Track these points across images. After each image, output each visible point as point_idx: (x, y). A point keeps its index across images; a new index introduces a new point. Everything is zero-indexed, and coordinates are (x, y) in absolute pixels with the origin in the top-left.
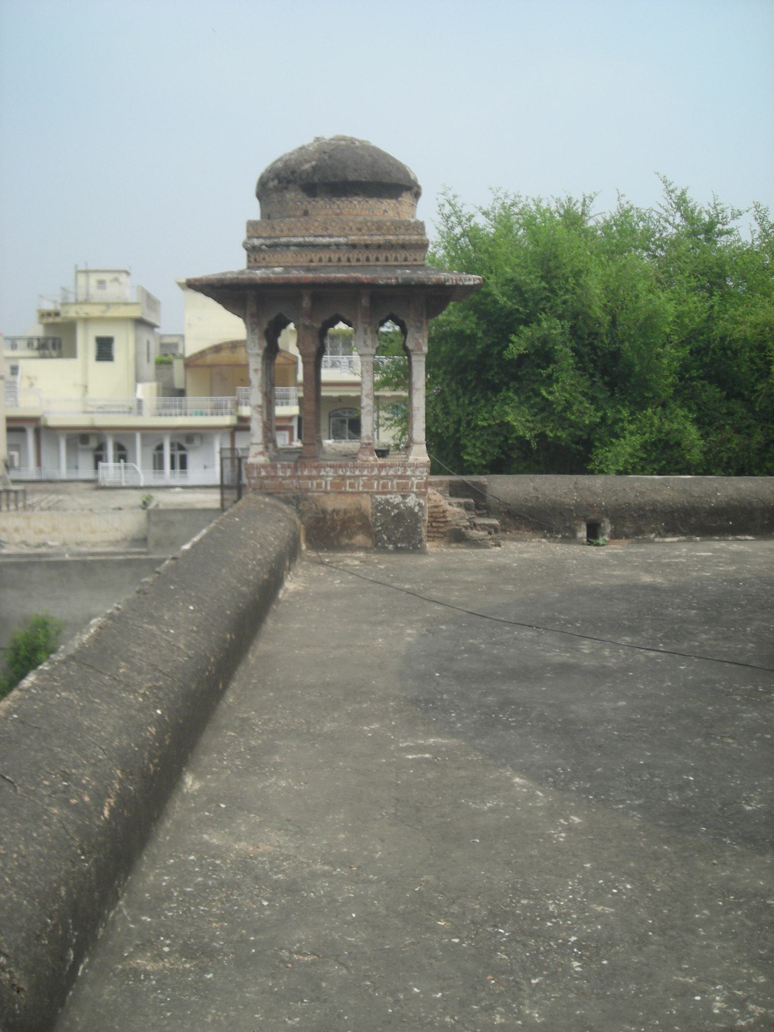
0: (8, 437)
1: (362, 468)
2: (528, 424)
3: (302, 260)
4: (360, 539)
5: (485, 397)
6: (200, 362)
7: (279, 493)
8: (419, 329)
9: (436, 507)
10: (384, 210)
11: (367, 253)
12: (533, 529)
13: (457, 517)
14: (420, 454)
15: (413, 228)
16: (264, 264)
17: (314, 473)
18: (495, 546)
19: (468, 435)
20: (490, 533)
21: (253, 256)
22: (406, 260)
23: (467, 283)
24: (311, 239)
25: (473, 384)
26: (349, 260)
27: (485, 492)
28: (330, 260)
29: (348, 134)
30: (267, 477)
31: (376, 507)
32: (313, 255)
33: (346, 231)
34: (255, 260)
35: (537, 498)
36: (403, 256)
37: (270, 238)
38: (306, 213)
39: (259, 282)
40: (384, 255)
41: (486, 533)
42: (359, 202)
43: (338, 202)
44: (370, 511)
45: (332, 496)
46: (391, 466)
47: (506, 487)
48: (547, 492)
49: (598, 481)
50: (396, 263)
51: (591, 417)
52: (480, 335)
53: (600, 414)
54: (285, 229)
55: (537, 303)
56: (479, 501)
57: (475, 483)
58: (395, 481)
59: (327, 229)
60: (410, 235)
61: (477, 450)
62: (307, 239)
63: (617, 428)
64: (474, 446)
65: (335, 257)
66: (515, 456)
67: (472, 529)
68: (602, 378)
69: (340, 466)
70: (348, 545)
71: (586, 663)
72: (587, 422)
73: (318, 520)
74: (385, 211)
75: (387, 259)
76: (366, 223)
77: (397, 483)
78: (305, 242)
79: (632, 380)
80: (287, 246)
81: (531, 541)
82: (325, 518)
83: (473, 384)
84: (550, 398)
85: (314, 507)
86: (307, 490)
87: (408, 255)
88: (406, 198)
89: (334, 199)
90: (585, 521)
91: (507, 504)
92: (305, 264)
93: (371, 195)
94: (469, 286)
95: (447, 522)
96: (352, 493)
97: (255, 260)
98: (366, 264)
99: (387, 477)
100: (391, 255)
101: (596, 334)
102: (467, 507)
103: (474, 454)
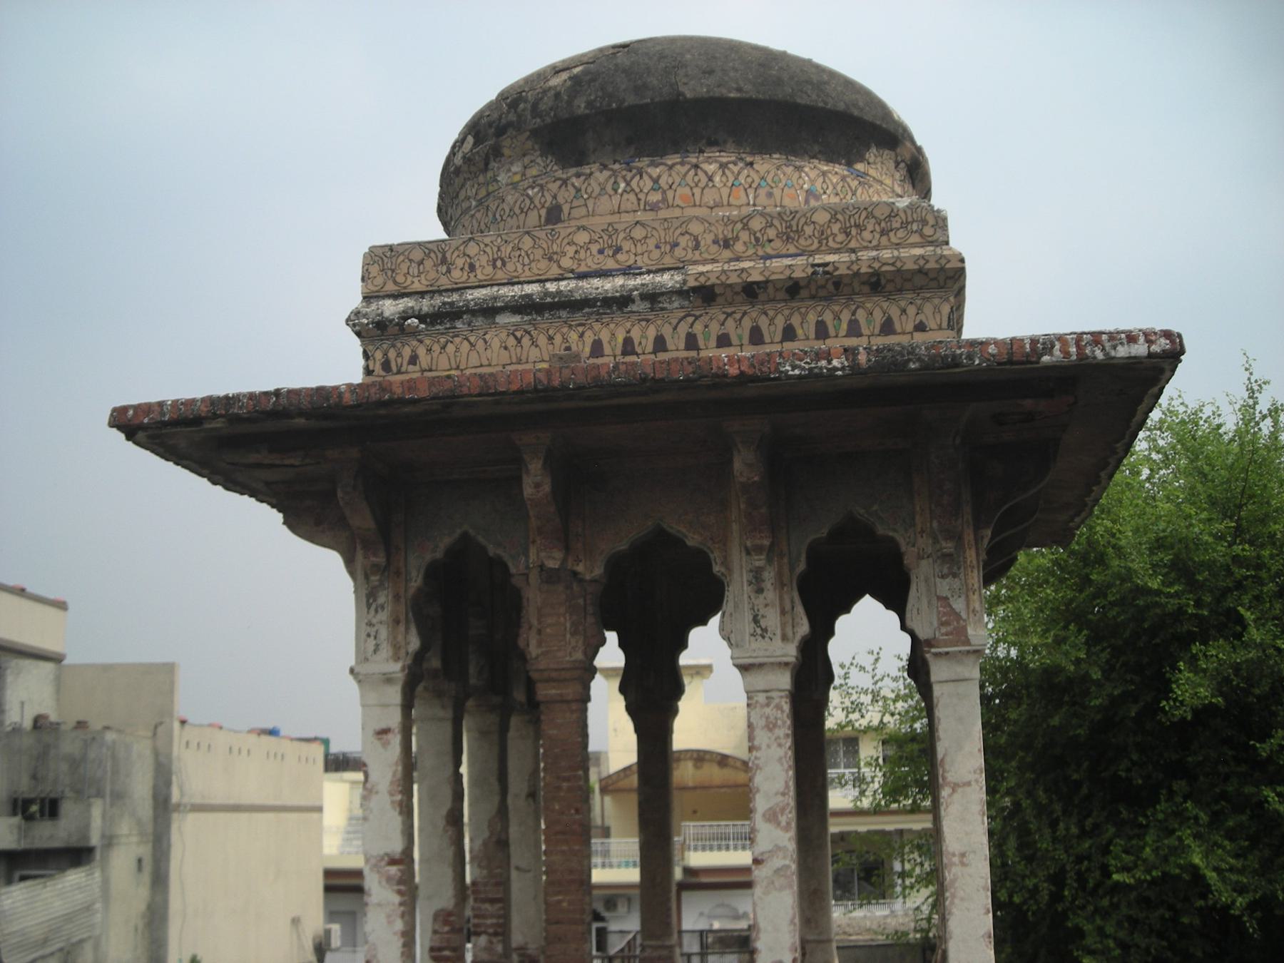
0: (326, 898)
2: (1234, 877)
3: (534, 354)
8: (951, 563)
15: (905, 225)
19: (1083, 908)
21: (379, 355)
23: (1122, 352)
25: (1084, 790)
32: (574, 336)
33: (678, 252)
34: (386, 366)
36: (878, 317)
39: (349, 399)
40: (812, 318)
42: (723, 166)
43: (655, 172)
52: (1096, 674)
59: (618, 250)
60: (898, 246)
61: (1111, 944)
62: (551, 287)
64: (1101, 931)
65: (644, 336)
74: (809, 193)
76: (745, 222)
78: (547, 294)
80: (489, 311)
87: (894, 312)
93: (763, 148)
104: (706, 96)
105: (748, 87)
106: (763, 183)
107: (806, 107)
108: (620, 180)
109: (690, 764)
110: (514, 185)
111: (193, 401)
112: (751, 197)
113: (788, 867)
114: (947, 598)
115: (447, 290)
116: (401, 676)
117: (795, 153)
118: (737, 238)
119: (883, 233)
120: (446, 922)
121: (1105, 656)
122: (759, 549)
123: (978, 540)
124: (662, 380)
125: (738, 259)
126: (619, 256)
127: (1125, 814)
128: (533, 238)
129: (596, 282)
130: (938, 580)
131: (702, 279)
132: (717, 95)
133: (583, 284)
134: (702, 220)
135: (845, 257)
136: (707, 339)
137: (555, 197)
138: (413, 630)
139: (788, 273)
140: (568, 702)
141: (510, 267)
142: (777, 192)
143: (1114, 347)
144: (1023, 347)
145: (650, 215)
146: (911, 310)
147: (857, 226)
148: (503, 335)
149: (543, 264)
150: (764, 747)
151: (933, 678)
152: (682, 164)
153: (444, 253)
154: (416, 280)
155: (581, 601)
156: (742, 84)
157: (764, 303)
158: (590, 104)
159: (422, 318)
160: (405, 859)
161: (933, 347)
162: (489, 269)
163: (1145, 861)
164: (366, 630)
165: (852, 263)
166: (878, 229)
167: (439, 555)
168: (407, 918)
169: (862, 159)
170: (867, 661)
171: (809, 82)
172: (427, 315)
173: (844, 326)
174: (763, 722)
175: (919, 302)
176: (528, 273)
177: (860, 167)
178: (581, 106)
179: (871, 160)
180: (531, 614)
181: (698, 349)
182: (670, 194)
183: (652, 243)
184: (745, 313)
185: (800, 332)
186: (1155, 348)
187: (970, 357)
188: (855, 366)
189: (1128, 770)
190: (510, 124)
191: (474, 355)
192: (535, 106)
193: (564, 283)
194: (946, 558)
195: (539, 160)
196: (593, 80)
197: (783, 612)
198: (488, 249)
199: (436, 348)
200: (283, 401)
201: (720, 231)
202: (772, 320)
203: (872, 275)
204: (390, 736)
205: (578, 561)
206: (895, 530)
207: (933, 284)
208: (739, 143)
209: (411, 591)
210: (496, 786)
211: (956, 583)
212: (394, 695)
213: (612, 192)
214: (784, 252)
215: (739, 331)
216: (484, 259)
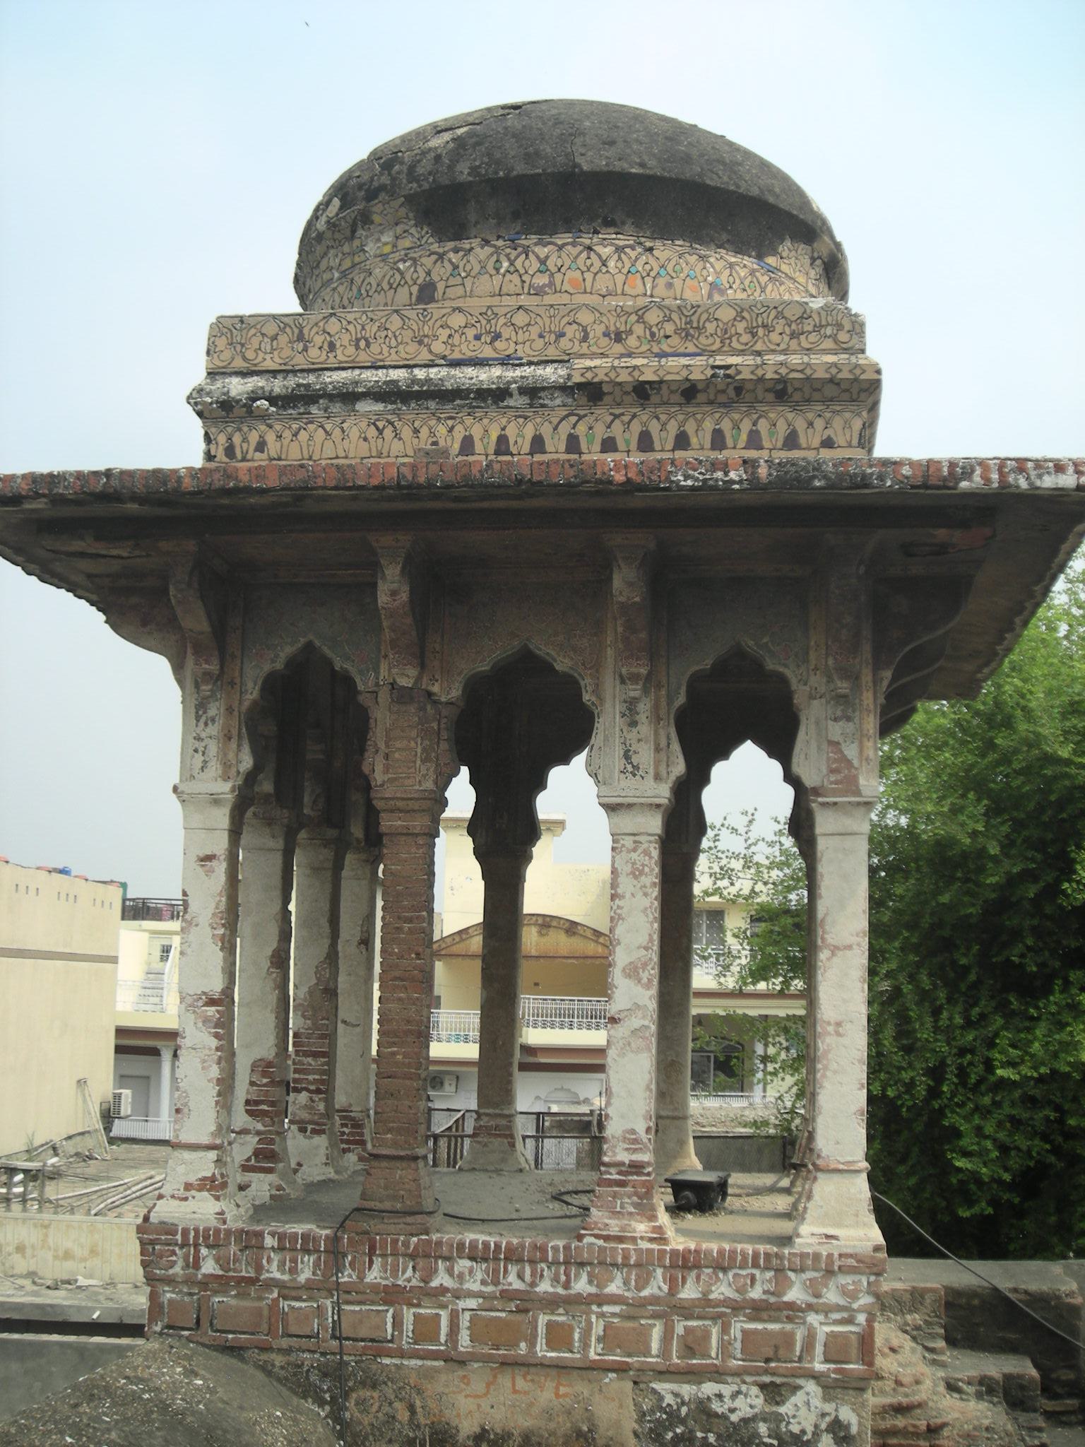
0: (116, 1059)
1: (603, 1265)
3: (397, 447)
5: (1003, 1007)
7: (265, 1349)
8: (845, 705)
9: (900, 1409)
11: (644, 419)
14: (841, 1212)
15: (818, 328)
17: (408, 1277)
21: (222, 439)
23: (1048, 482)
25: (972, 977)
27: (1075, 1332)
30: (220, 1283)
32: (442, 430)
33: (564, 343)
34: (230, 451)
39: (188, 485)
40: (709, 425)
42: (620, 250)
43: (543, 251)
45: (478, 1376)
46: (722, 1265)
52: (994, 849)
58: (739, 1326)
59: (497, 336)
61: (989, 1144)
62: (420, 374)
64: (979, 1131)
69: (513, 1256)
76: (640, 313)
77: (744, 1331)
78: (414, 381)
80: (348, 397)
83: (972, 977)
85: (404, 1416)
86: (378, 1346)
87: (800, 425)
93: (665, 232)
94: (1060, 493)
96: (560, 1368)
97: (230, 451)
99: (703, 1308)
102: (1012, 1395)
103: (982, 1153)
104: (605, 169)
105: (652, 163)
106: (663, 272)
107: (717, 189)
108: (502, 258)
109: (534, 930)
110: (383, 257)
111: (13, 477)
112: (649, 286)
113: (647, 1027)
114: (838, 743)
115: (302, 371)
116: (230, 797)
118: (630, 332)
119: (793, 335)
120: (264, 1074)
121: (1005, 829)
122: (634, 678)
123: (876, 682)
124: (540, 482)
125: (630, 355)
126: (497, 344)
127: (1015, 1004)
128: (402, 317)
129: (470, 371)
130: (830, 722)
131: (589, 375)
132: (618, 169)
133: (456, 372)
134: (593, 309)
135: (750, 360)
136: (590, 442)
137: (428, 273)
139: (684, 373)
140: (417, 835)
141: (375, 348)
142: (677, 283)
143: (1040, 476)
144: (940, 470)
145: (535, 300)
146: (819, 424)
147: (764, 326)
148: (364, 425)
149: (412, 348)
150: (628, 895)
151: (818, 830)
152: (574, 244)
153: (301, 329)
154: (268, 357)
155: (435, 725)
156: (646, 158)
157: (656, 405)
158: (474, 170)
159: (272, 400)
160: (223, 1000)
161: (841, 463)
162: (351, 350)
163: (1032, 1056)
164: (193, 746)
165: (757, 366)
166: (787, 330)
167: (279, 666)
168: (223, 1063)
169: (774, 252)
170: (740, 822)
171: (721, 161)
172: (279, 397)
173: (744, 437)
174: (628, 868)
175: (828, 415)
176: (394, 356)
177: (771, 260)
178: (463, 172)
179: (784, 254)
180: (378, 736)
181: (580, 453)
182: (558, 277)
183: (535, 331)
184: (634, 416)
185: (694, 441)
187: (881, 478)
188: (754, 481)
189: (1022, 956)
190: (382, 188)
191: (329, 444)
192: (412, 169)
193: (434, 370)
194: (842, 699)
195: (413, 230)
196: (478, 144)
197: (658, 749)
198: (351, 327)
199: (287, 434)
201: (613, 323)
202: (664, 425)
203: (778, 381)
204: (214, 863)
205: (435, 680)
206: (786, 666)
207: (846, 396)
208: (638, 225)
209: (246, 704)
210: (327, 930)
212: (221, 818)
213: (494, 272)
214: (682, 350)
215: (627, 435)
216: (346, 338)
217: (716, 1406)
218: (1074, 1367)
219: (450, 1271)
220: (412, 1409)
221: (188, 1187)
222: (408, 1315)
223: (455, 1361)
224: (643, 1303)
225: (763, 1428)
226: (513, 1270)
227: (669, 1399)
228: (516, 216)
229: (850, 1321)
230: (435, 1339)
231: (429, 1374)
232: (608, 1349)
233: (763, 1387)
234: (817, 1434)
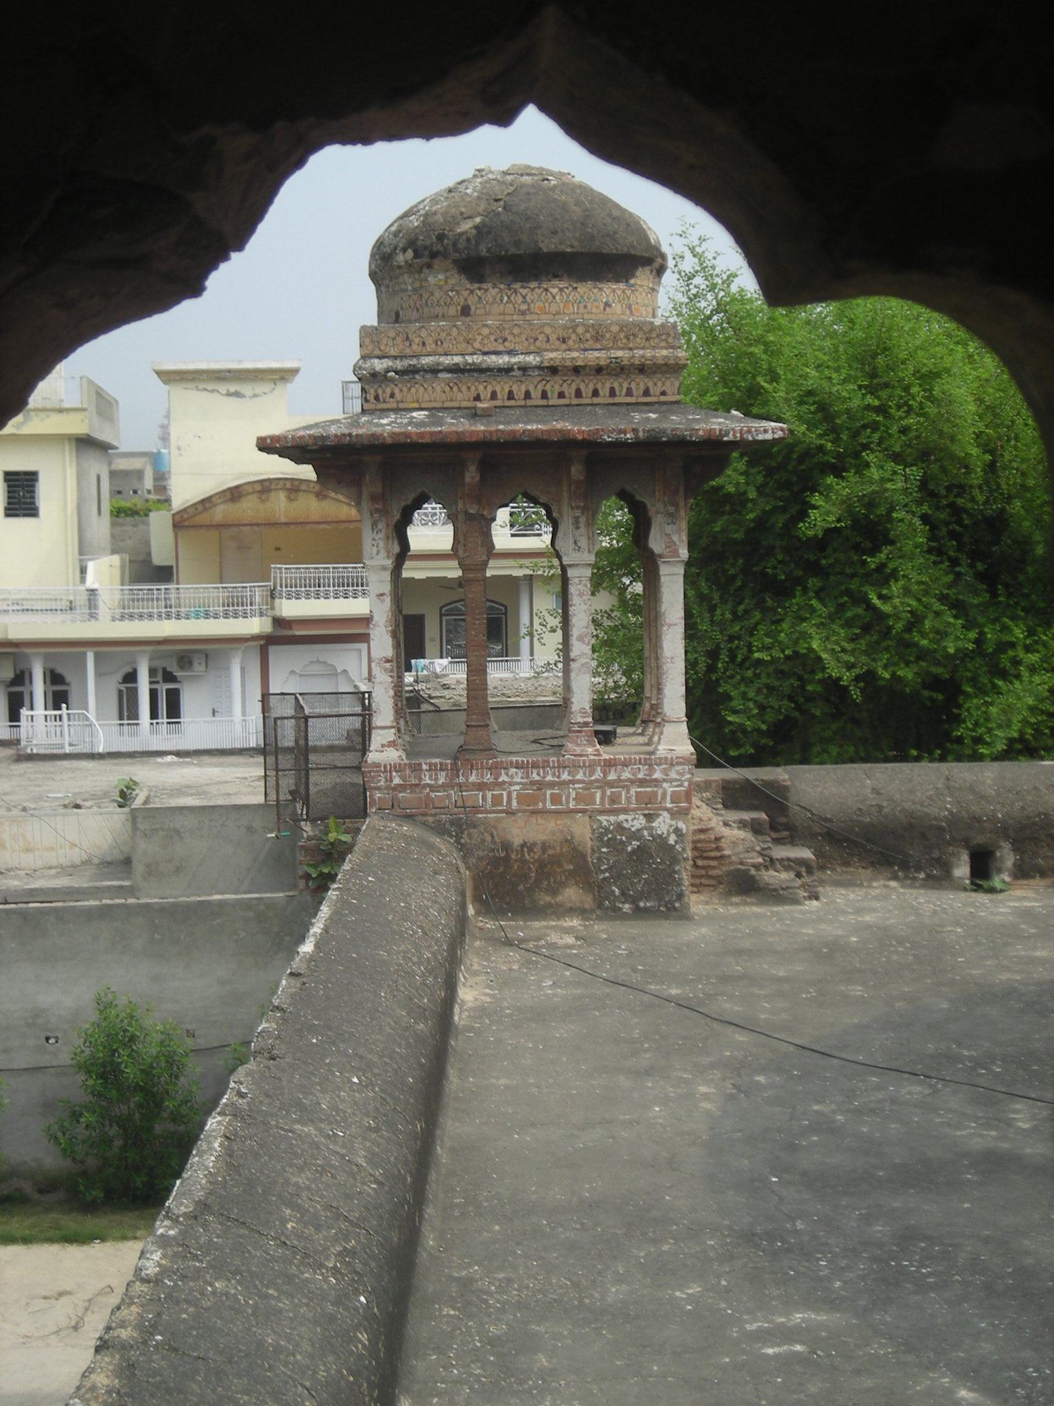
1: (575, 767)
2: (846, 657)
3: (460, 396)
4: (572, 894)
5: (760, 606)
6: (203, 519)
7: (424, 815)
8: (672, 518)
9: (702, 831)
10: (604, 301)
11: (577, 382)
12: (873, 864)
13: (741, 848)
14: (675, 740)
15: (658, 336)
16: (394, 405)
17: (488, 778)
18: (810, 898)
19: (732, 677)
20: (799, 875)
21: (372, 391)
22: (646, 393)
23: (760, 437)
24: (477, 359)
25: (738, 583)
26: (544, 395)
27: (786, 799)
28: (511, 396)
29: (535, 162)
30: (402, 788)
31: (601, 836)
32: (481, 387)
33: (538, 343)
34: (377, 398)
35: (880, 807)
36: (642, 387)
37: (402, 357)
38: (465, 311)
39: (389, 441)
40: (608, 385)
41: (792, 875)
42: (561, 290)
43: (524, 292)
44: (589, 843)
46: (625, 764)
47: (827, 786)
48: (898, 796)
49: (988, 774)
50: (629, 400)
51: (957, 641)
52: (752, 494)
53: (973, 635)
54: (429, 341)
55: (855, 434)
56: (775, 815)
57: (770, 784)
59: (505, 340)
60: (654, 348)
61: (751, 705)
62: (469, 359)
63: (1004, 660)
64: (744, 696)
66: (818, 713)
67: (767, 868)
68: (972, 566)
69: (535, 765)
70: (550, 905)
71: (1028, 1151)
72: (951, 651)
73: (495, 862)
74: (607, 305)
75: (612, 393)
78: (467, 364)
79: (1030, 569)
80: (434, 371)
81: (870, 887)
82: (508, 855)
83: (738, 583)
84: (886, 608)
85: (489, 839)
86: (476, 809)
87: (650, 385)
88: (642, 278)
89: (517, 286)
90: (967, 847)
91: (826, 820)
92: (465, 404)
93: (582, 279)
95: (722, 857)
97: (377, 398)
98: (575, 401)
99: (617, 783)
100: (621, 385)
101: (961, 487)
103: (746, 711)
105: (576, 244)
109: (282, 495)
110: (440, 287)
117: (599, 280)
122: (578, 507)
123: (686, 504)
127: (770, 603)
129: (493, 357)
136: (553, 392)
138: (396, 542)
142: (589, 305)
145: (521, 317)
146: (659, 384)
149: (464, 345)
158: (489, 250)
159: (396, 373)
162: (434, 346)
163: (780, 642)
171: (608, 235)
178: (483, 250)
183: (523, 337)
185: (601, 392)
186: (776, 436)
189: (775, 568)
192: (455, 244)
194: (670, 515)
199: (405, 389)
200: (354, 439)
201: (561, 333)
211: (675, 527)
217: (625, 825)
218: (787, 816)
219: (507, 774)
220: (492, 836)
221: (383, 746)
222: (489, 795)
223: (513, 813)
224: (592, 782)
225: (645, 833)
226: (535, 771)
227: (605, 823)
228: (510, 273)
229: (681, 785)
230: (501, 804)
231: (498, 820)
232: (578, 803)
233: (645, 815)
234: (668, 834)
